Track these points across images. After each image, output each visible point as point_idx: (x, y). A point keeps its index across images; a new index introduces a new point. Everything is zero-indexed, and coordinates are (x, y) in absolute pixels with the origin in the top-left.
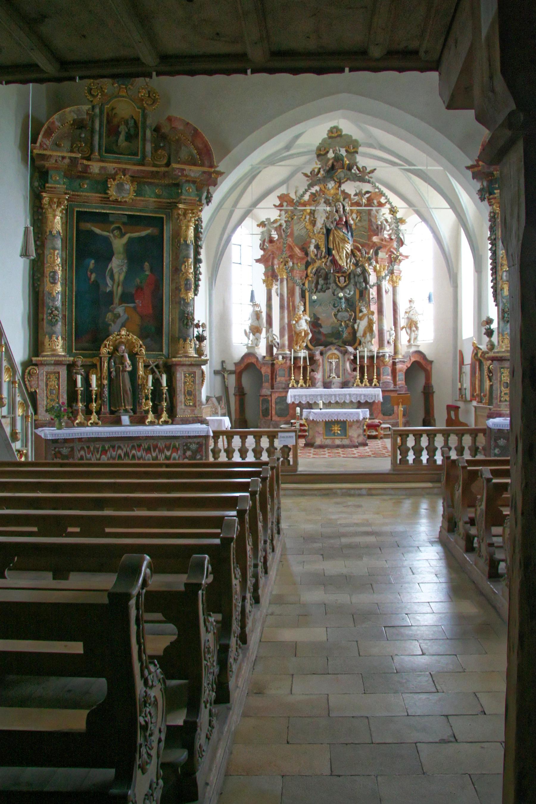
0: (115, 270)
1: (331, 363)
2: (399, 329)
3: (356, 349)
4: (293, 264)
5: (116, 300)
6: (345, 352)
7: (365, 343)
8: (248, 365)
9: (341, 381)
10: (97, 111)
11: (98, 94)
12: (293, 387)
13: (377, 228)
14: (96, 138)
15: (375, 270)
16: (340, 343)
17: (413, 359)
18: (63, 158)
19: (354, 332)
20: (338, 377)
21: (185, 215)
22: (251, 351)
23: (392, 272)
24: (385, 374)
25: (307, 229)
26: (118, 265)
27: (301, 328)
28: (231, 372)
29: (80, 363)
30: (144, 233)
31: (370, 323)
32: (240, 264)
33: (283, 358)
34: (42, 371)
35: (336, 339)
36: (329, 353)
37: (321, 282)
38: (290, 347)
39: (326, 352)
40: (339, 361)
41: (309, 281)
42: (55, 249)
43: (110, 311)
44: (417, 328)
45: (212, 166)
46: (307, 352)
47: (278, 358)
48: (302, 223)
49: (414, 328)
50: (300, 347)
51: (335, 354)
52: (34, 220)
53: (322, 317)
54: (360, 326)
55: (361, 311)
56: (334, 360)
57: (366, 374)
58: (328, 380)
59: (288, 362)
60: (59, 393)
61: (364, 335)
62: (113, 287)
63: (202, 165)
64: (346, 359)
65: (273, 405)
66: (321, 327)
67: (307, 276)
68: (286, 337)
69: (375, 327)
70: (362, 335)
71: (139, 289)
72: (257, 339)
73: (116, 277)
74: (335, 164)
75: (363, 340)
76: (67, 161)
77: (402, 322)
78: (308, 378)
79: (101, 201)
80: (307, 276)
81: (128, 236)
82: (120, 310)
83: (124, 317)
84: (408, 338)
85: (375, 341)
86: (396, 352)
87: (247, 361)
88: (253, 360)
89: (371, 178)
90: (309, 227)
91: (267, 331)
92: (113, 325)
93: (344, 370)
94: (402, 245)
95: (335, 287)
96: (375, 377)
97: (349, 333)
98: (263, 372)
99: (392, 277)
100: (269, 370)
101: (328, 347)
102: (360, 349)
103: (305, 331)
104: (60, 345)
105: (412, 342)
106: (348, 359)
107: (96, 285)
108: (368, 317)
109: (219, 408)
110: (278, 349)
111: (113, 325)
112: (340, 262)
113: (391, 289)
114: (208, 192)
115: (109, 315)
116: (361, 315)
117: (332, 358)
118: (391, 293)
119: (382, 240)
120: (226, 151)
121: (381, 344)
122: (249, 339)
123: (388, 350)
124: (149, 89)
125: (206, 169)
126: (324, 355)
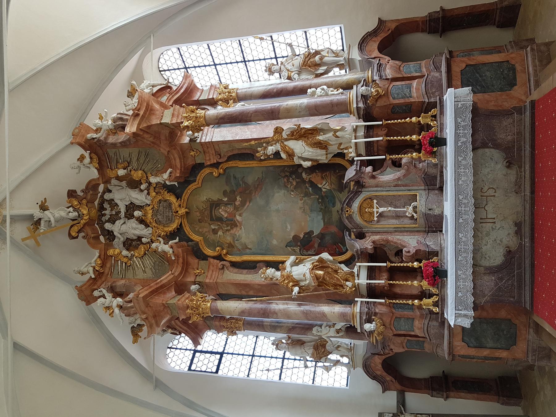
1: (381, 215)
3: (352, 162)
4: (195, 283)
7: (341, 144)
9: (424, 193)
16: (343, 196)
17: (376, 53)
19: (318, 167)
20: (414, 198)
22: (359, 361)
24: (407, 91)
25: (145, 254)
27: (308, 275)
28: (402, 402)
31: (300, 134)
32: (222, 354)
33: (369, 321)
35: (334, 205)
36: (358, 219)
38: (348, 301)
39: (357, 226)
40: (376, 197)
44: (317, 53)
46: (358, 264)
48: (134, 262)
49: (317, 58)
50: (347, 280)
51: (360, 207)
53: (291, 231)
54: (305, 155)
55: (277, 155)
56: (375, 210)
57: (408, 137)
58: (421, 221)
61: (322, 145)
64: (372, 182)
65: (486, 353)
67: (219, 258)
69: (308, 123)
70: (324, 152)
72: (339, 346)
75: (334, 149)
77: (305, 80)
78: (416, 264)
80: (219, 258)
84: (336, 70)
85: (334, 122)
87: (379, 370)
88: (378, 360)
93: (397, 184)
94: (170, 88)
96: (414, 119)
97: (322, 178)
98: (401, 350)
99: (221, 100)
101: (346, 222)
102: (351, 153)
103: (315, 268)
105: (341, 60)
106: (373, 177)
108: (286, 140)
116: (283, 156)
117: (372, 214)
119: (136, 115)
122: (337, 362)
126: (365, 230)
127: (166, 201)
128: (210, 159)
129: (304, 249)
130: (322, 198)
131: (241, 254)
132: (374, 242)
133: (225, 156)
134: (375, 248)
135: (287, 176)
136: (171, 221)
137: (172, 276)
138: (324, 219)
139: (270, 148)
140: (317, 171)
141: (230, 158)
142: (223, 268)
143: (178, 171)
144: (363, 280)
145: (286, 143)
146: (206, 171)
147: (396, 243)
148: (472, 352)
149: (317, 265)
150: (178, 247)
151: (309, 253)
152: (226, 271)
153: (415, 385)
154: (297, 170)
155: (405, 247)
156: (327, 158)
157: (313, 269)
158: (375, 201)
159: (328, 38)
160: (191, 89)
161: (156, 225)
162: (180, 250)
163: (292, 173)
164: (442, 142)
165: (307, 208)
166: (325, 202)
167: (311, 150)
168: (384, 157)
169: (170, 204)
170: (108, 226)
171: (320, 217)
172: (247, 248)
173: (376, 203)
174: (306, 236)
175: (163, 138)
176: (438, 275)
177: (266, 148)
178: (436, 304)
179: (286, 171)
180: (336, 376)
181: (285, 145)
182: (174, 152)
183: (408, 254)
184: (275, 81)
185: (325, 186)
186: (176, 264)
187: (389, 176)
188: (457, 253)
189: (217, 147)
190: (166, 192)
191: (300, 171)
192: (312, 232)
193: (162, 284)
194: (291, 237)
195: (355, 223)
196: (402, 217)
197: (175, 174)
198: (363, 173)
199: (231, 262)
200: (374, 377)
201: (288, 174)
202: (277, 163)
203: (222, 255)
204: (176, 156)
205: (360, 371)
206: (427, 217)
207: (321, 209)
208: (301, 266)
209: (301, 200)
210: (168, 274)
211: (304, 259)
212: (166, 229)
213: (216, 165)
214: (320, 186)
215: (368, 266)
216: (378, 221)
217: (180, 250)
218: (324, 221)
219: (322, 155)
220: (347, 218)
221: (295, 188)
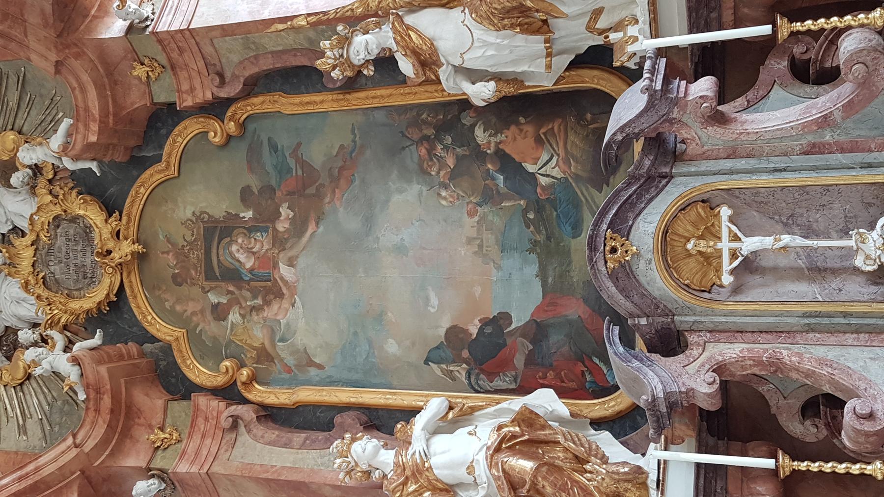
1: (748, 266)
4: (147, 472)
7: (598, 13)
19: (520, 105)
27: (482, 471)
36: (654, 279)
40: (730, 195)
41: (254, 378)
51: (666, 234)
53: (441, 313)
54: (475, 60)
55: (385, 63)
64: (715, 135)
66: (504, 318)
67: (229, 393)
70: (536, 43)
75: (575, 36)
80: (229, 393)
97: (539, 141)
101: (610, 290)
116: (406, 66)
117: (710, 260)
127: (75, 219)
128: (192, 89)
129: (482, 371)
130: (538, 206)
131: (294, 383)
132: (719, 369)
133: (235, 77)
134: (725, 387)
135: (426, 138)
136: (89, 279)
137: (74, 452)
138: (542, 274)
139: (359, 40)
140: (522, 120)
141: (254, 86)
142: (234, 426)
143: (95, 127)
145: (409, 20)
146: (189, 128)
147: (809, 374)
149: (514, 436)
150: (100, 362)
151: (498, 383)
152: (244, 437)
154: (458, 118)
155: (854, 394)
156: (549, 67)
157: (498, 449)
158: (725, 212)
161: (45, 293)
162: (103, 370)
163: (442, 129)
165: (489, 238)
166: (547, 223)
167: (492, 37)
168: (766, 30)
169: (87, 231)
171: (532, 269)
172: (311, 363)
173: (731, 220)
174: (488, 330)
175: (33, 19)
177: (345, 41)
179: (425, 122)
181: (408, 28)
182: (76, 64)
183: (868, 427)
186: (91, 414)
187: (781, 113)
189: (208, 49)
190: (74, 193)
191: (467, 120)
192: (504, 318)
193: (37, 478)
194: (442, 332)
195: (645, 295)
196: (834, 272)
197: (85, 137)
198: (676, 102)
199: (263, 406)
201: (430, 132)
202: (394, 97)
203: (239, 384)
204: (85, 78)
207: (535, 243)
209: (471, 214)
210: (63, 447)
211: (473, 409)
212: (75, 305)
213: (216, 108)
214: (531, 168)
215: (698, 466)
216: (737, 289)
217: (103, 370)
218: (544, 284)
219: (533, 58)
220: (613, 276)
221: (454, 175)
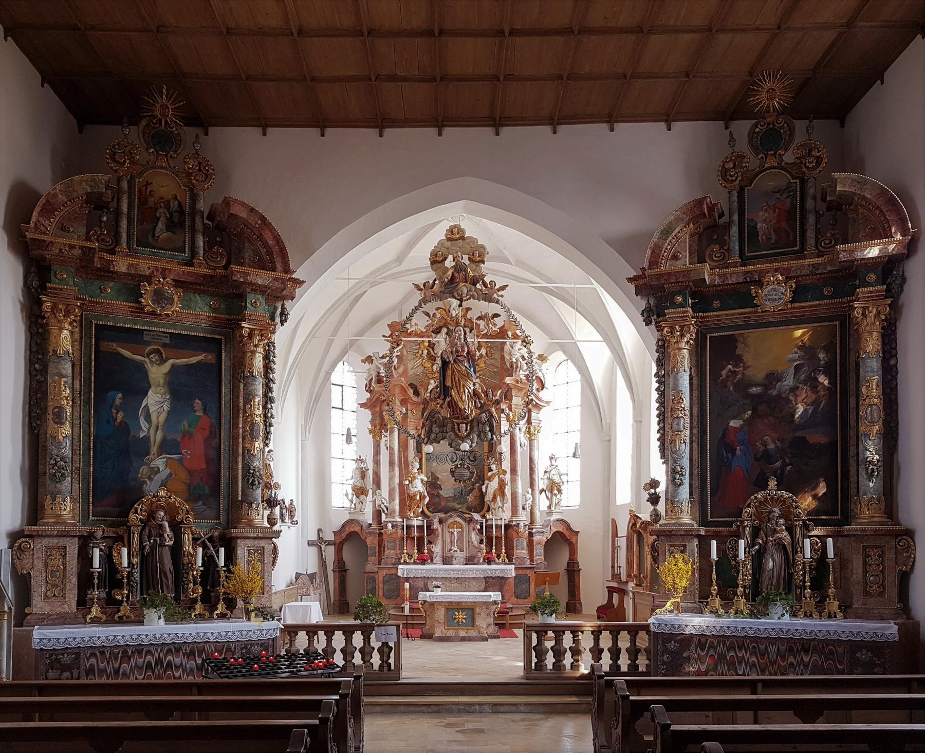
0: (152, 409)
1: (452, 533)
2: (537, 492)
3: (483, 516)
5: (154, 450)
6: (470, 521)
8: (349, 536)
10: (125, 185)
11: (125, 162)
12: (405, 563)
13: (512, 367)
14: (124, 223)
15: (508, 419)
17: (554, 530)
18: (72, 247)
19: (482, 495)
20: (462, 551)
21: (251, 335)
22: (355, 517)
23: (529, 422)
26: (156, 401)
27: (416, 490)
28: (329, 543)
29: (99, 534)
30: (193, 360)
31: (502, 485)
33: (393, 526)
34: (40, 545)
36: (451, 520)
37: (435, 429)
38: (403, 514)
39: (446, 520)
42: (61, 376)
43: (144, 464)
44: (560, 491)
45: (287, 270)
47: (386, 527)
49: (556, 492)
52: (31, 333)
55: (490, 470)
58: (449, 555)
59: (399, 532)
60: (64, 576)
62: (149, 430)
63: (274, 269)
68: (397, 501)
71: (187, 435)
73: (154, 418)
74: (456, 275)
75: (492, 506)
76: (77, 252)
77: (541, 484)
79: (131, 312)
81: (171, 361)
82: (159, 463)
83: (164, 472)
84: (548, 503)
85: (508, 505)
86: (532, 521)
87: (348, 530)
88: (357, 529)
89: (502, 296)
90: (428, 365)
91: (374, 493)
92: (148, 482)
93: (470, 541)
95: (453, 437)
100: (376, 542)
104: (68, 509)
105: (553, 508)
107: (124, 429)
109: (312, 589)
110: (386, 514)
111: (148, 482)
112: (460, 405)
113: (527, 443)
114: (283, 308)
115: (144, 470)
116: (490, 474)
118: (526, 448)
120: (308, 252)
121: (515, 512)
123: (523, 518)
124: (200, 160)
125: (278, 274)
144: (416, 522)
148: (381, 579)
153: (339, 552)
159: (571, 497)
160: (538, 407)
164: (489, 563)
166: (460, 496)
170: (444, 330)
176: (423, 561)
178: (405, 561)
180: (341, 498)
184: (542, 465)
185: (470, 498)
187: (475, 538)
188: (434, 570)
200: (343, 526)
205: (347, 517)
206: (452, 557)
208: (421, 485)
